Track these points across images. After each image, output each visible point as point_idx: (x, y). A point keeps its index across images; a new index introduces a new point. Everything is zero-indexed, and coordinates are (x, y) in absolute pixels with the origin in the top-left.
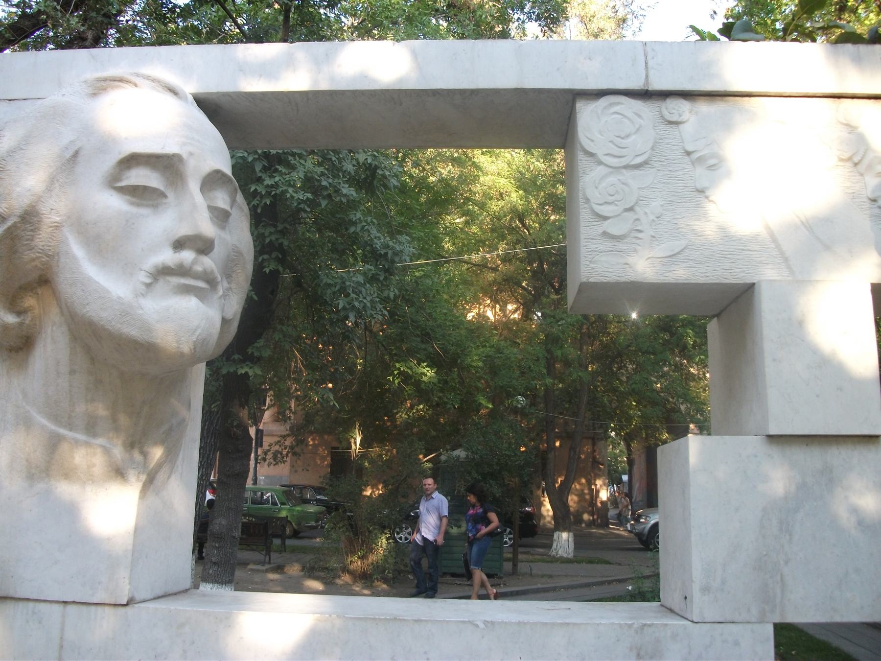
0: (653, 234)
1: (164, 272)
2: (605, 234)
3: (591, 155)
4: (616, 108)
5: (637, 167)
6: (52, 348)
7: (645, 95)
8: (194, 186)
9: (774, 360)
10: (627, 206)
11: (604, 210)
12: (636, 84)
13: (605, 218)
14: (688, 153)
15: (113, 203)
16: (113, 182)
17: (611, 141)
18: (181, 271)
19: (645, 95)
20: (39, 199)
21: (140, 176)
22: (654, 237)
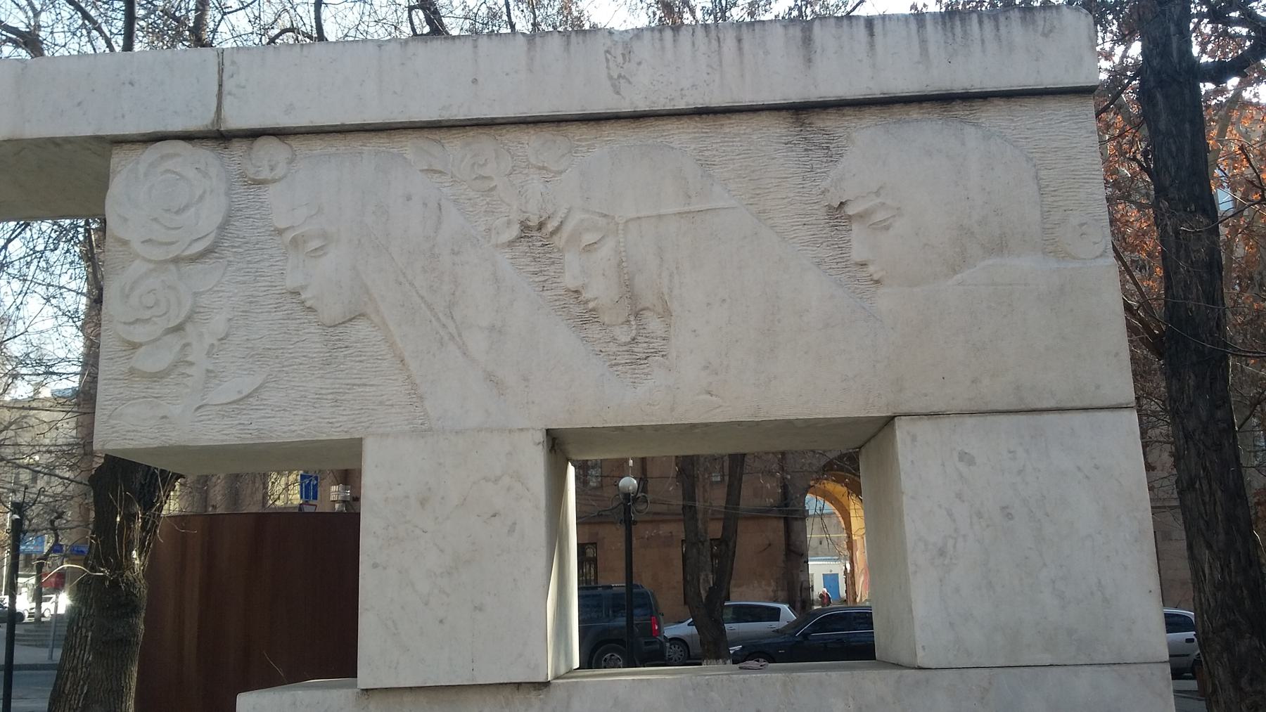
0: (211, 368)
2: (132, 372)
3: (126, 243)
4: (169, 164)
5: (194, 259)
7: (220, 137)
9: (375, 566)
10: (171, 325)
12: (200, 120)
13: (135, 346)
14: (280, 232)
17: (155, 220)
19: (220, 137)
22: (211, 371)
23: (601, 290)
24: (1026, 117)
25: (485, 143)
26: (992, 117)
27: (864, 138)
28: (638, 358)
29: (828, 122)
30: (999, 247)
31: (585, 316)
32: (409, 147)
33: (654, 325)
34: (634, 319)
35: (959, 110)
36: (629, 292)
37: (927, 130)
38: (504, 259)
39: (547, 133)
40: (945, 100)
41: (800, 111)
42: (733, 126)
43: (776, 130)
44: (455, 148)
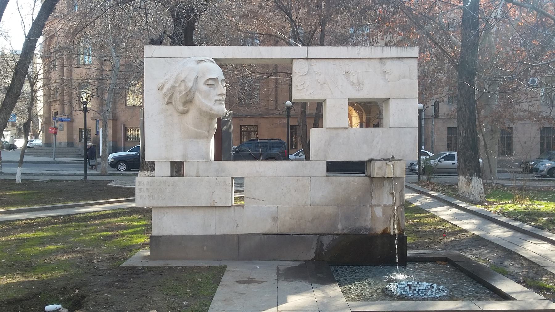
1: (217, 100)
6: (192, 114)
7: (307, 59)
8: (220, 83)
11: (298, 84)
12: (305, 57)
15: (205, 88)
16: (206, 83)
18: (220, 100)
19: (307, 59)
20: (192, 87)
21: (210, 82)
23: (355, 81)
24: (409, 60)
25: (341, 61)
26: (405, 60)
27: (389, 62)
28: (359, 90)
29: (384, 60)
30: (404, 78)
31: (353, 84)
32: (331, 61)
33: (361, 86)
34: (359, 85)
35: (401, 59)
36: (359, 81)
37: (397, 62)
38: (343, 76)
39: (349, 60)
40: (399, 58)
41: (381, 58)
42: (372, 60)
43: (378, 61)
44: (337, 61)
